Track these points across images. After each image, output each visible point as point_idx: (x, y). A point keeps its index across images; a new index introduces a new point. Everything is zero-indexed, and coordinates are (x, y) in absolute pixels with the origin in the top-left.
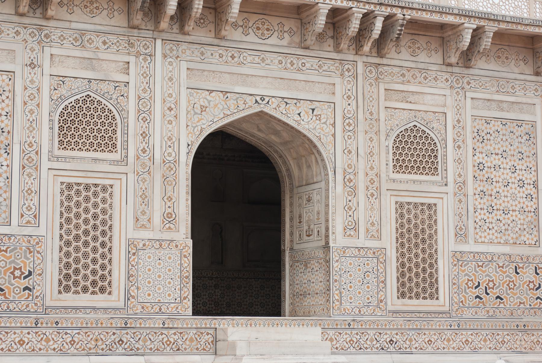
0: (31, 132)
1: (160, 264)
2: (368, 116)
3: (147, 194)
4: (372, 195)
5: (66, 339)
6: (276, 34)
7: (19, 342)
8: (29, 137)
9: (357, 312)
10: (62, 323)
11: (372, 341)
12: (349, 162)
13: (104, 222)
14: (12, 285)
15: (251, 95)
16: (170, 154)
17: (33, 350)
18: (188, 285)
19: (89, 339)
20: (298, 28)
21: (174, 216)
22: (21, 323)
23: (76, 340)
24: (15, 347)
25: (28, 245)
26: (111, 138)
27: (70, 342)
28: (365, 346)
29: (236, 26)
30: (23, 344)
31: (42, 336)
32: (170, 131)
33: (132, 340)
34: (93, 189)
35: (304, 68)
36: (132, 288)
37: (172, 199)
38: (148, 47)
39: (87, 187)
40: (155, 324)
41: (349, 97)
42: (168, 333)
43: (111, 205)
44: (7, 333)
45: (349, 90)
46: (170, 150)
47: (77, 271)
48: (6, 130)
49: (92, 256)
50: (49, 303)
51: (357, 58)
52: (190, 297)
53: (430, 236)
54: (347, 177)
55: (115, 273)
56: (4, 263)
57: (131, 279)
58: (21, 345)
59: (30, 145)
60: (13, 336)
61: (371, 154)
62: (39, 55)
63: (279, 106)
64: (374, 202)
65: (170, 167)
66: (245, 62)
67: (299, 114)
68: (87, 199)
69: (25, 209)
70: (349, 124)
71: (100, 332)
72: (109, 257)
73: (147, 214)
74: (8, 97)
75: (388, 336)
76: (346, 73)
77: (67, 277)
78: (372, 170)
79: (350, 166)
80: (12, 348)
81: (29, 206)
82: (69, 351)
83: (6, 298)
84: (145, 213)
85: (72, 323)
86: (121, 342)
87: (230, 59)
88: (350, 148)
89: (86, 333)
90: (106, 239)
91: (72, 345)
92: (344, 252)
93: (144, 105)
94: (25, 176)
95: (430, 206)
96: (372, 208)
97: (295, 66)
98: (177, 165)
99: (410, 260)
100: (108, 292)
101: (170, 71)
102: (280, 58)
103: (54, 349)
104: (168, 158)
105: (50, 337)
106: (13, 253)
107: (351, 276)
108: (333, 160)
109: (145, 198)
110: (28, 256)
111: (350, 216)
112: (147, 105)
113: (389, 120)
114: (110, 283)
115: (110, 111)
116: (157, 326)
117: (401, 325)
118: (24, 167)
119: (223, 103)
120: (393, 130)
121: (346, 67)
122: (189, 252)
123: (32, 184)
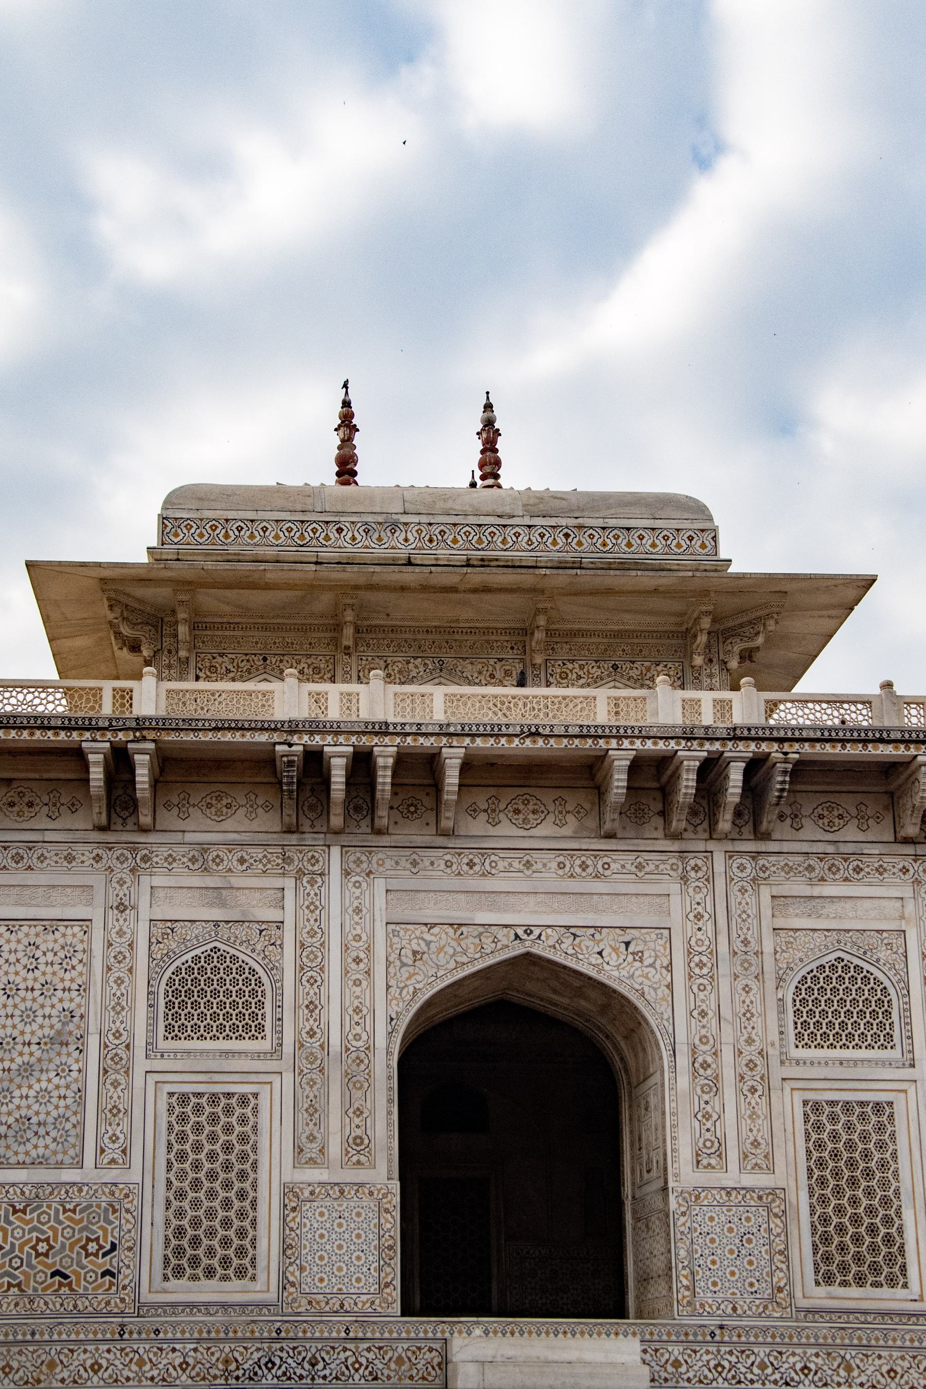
0: (118, 1013)
1: (340, 1225)
2: (738, 945)
3: (317, 1106)
4: (753, 1090)
5: (174, 1359)
6: (551, 818)
7: (92, 1366)
8: (114, 1022)
9: (729, 1311)
10: (166, 1332)
11: (762, 1366)
12: (703, 1032)
13: (243, 1157)
14: (83, 1268)
15: (506, 926)
16: (357, 1037)
17: (116, 1381)
18: (392, 1262)
19: (214, 1359)
20: (593, 804)
21: (366, 1141)
22: (95, 1333)
23: (191, 1361)
24: (85, 1375)
25: (112, 1199)
26: (254, 1016)
27: (180, 1365)
28: (749, 1376)
29: (475, 811)
30: (99, 1370)
31: (131, 1355)
32: (358, 997)
33: (290, 1361)
34: (223, 1101)
35: (607, 873)
36: (291, 1269)
37: (362, 1113)
38: (318, 861)
39: (214, 1099)
40: (330, 1332)
41: (698, 917)
42: (357, 1348)
43: (255, 1128)
44: (72, 1351)
45: (698, 904)
46: (358, 1030)
47: (195, 1242)
48: (77, 1014)
49: (221, 1214)
50: (146, 1296)
51: (711, 845)
52: (397, 1283)
53: (883, 1165)
54: (700, 1059)
55: (262, 1244)
56: (71, 1231)
57: (289, 1252)
58: (96, 1372)
59: (117, 1035)
60: (82, 1356)
61: (748, 1014)
62: (132, 889)
63: (560, 942)
64: (757, 1104)
65: (358, 1058)
66: (493, 871)
67: (600, 953)
68: (214, 1119)
69: (106, 1141)
70: (701, 965)
71: (233, 1346)
72: (251, 1214)
73: (319, 1140)
74: (81, 961)
75: (797, 1358)
76: (693, 874)
77: (179, 1252)
78: (750, 1045)
79: (704, 1040)
80: (80, 1377)
81: (114, 1135)
82: (178, 1382)
83: (72, 1290)
84: (315, 1138)
85: (183, 1332)
86: (270, 1365)
87: (465, 868)
88: (704, 1007)
89: (209, 1348)
90: (247, 1185)
91: (184, 1370)
92: (697, 1197)
93: (312, 956)
94: (108, 1086)
95: (878, 1107)
96: (754, 1113)
97: (590, 870)
98: (371, 1055)
99: (839, 1210)
100: (249, 1275)
101: (357, 898)
102: (561, 859)
103: (152, 1379)
104: (354, 1043)
105: (145, 1357)
106: (85, 1214)
107: (713, 1241)
108: (671, 1031)
109: (314, 1111)
110: (111, 1217)
111: (708, 1130)
112: (316, 957)
113: (783, 951)
114: (253, 1261)
115: (253, 971)
116: (334, 1335)
117: (825, 1338)
118: (106, 1072)
119: (454, 944)
120: (792, 969)
121: (692, 863)
122: (394, 1202)
123: (119, 1097)
